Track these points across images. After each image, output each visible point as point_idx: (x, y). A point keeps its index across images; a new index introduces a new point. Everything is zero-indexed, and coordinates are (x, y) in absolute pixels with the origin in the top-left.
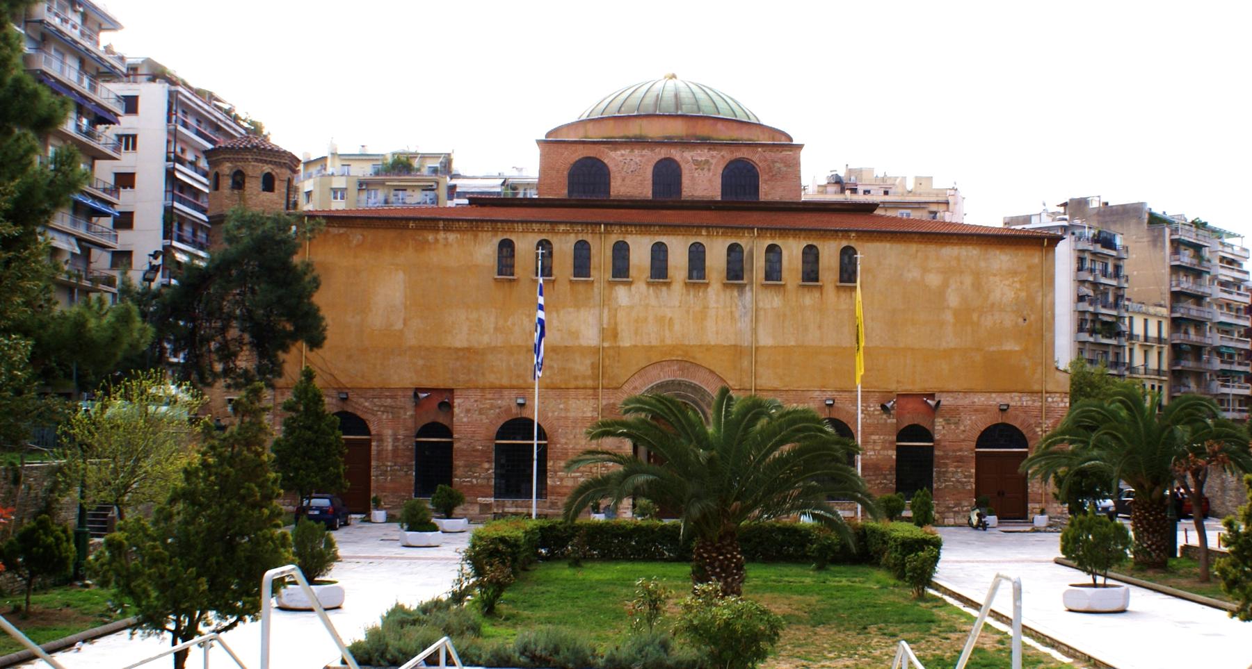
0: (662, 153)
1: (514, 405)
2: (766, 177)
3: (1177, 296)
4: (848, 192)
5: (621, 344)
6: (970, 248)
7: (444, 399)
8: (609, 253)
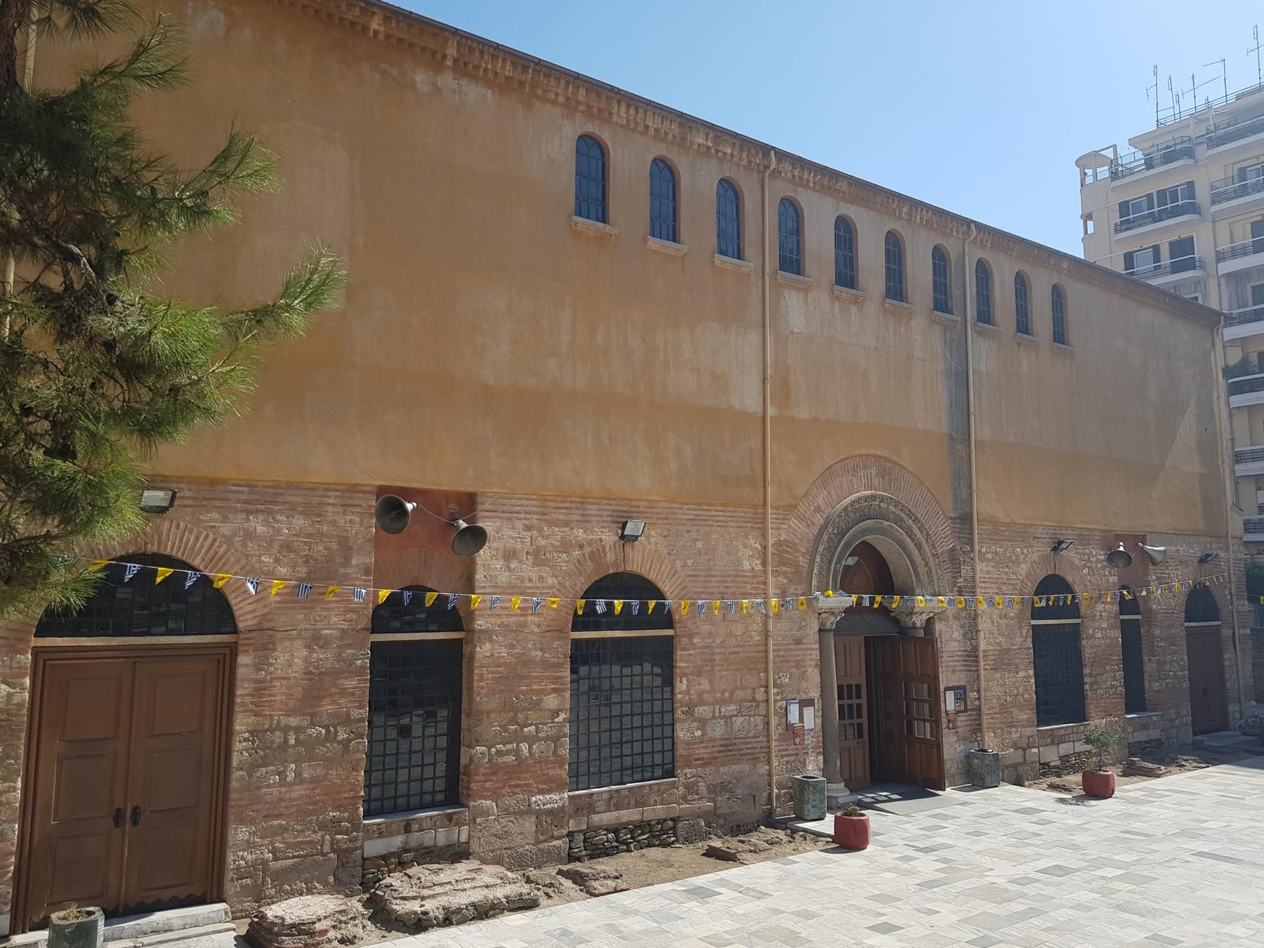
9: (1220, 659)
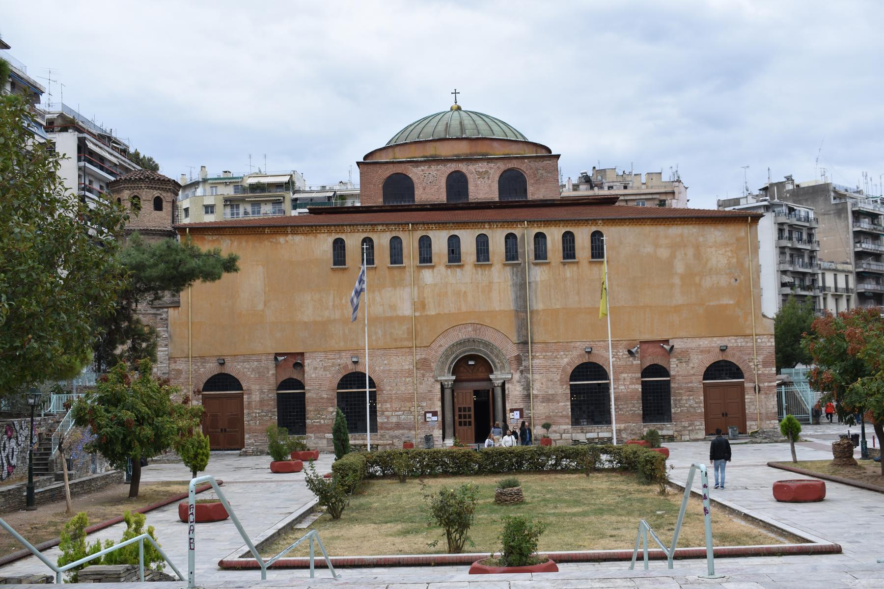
0: (452, 167)
1: (349, 362)
2: (532, 181)
3: (860, 256)
4: (596, 188)
5: (429, 313)
6: (690, 227)
7: (297, 360)
8: (416, 245)
9: (743, 399)
